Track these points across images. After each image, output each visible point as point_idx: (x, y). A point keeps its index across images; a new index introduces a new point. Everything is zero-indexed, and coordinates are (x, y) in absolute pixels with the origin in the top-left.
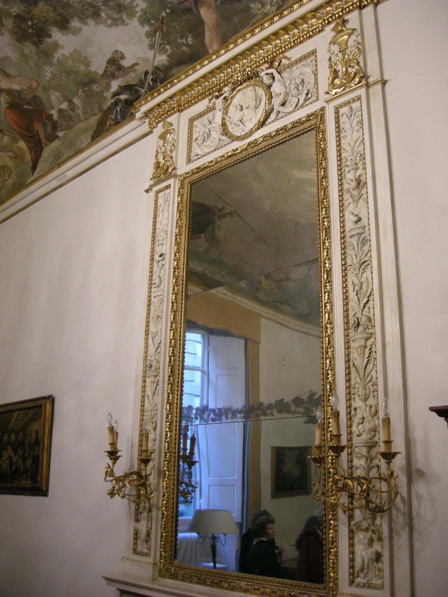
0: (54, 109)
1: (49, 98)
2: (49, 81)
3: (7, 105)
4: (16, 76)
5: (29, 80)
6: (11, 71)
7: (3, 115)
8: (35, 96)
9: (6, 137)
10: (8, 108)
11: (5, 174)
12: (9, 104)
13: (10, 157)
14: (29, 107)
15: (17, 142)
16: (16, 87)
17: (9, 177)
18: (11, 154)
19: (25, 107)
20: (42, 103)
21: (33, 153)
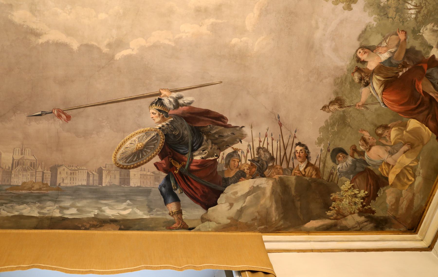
0: (431, 47)
1: (423, 38)
2: (416, 18)
3: (382, 88)
4: (381, 43)
5: (394, 37)
6: (374, 41)
7: (382, 104)
8: (407, 51)
9: (393, 129)
10: (383, 91)
11: (408, 179)
12: (383, 86)
13: (405, 152)
14: (404, 71)
15: (405, 125)
16: (385, 56)
17: (415, 176)
18: (406, 148)
19: (401, 74)
20: (417, 53)
21: (431, 124)
